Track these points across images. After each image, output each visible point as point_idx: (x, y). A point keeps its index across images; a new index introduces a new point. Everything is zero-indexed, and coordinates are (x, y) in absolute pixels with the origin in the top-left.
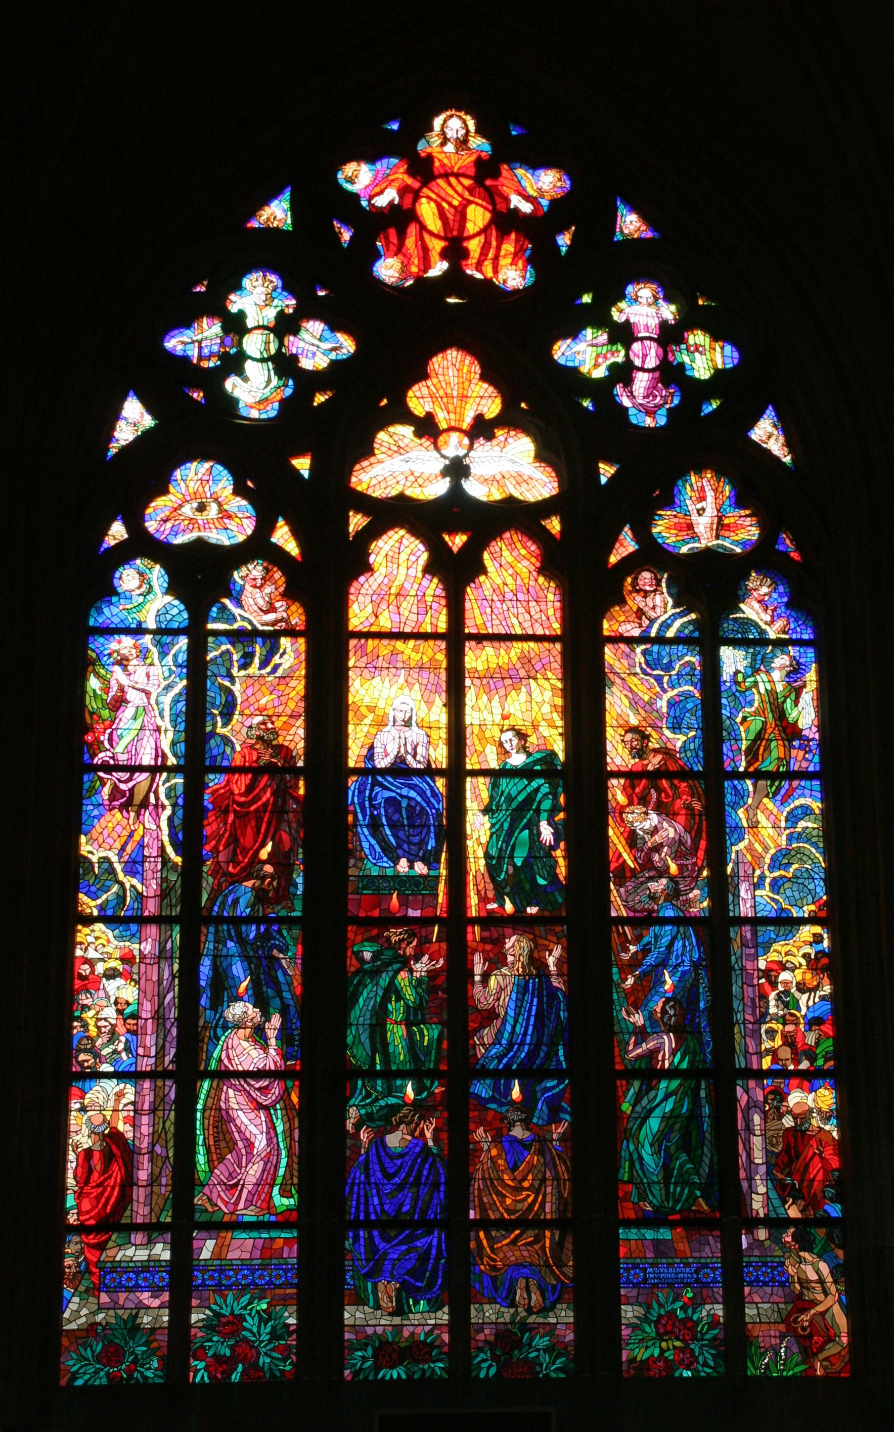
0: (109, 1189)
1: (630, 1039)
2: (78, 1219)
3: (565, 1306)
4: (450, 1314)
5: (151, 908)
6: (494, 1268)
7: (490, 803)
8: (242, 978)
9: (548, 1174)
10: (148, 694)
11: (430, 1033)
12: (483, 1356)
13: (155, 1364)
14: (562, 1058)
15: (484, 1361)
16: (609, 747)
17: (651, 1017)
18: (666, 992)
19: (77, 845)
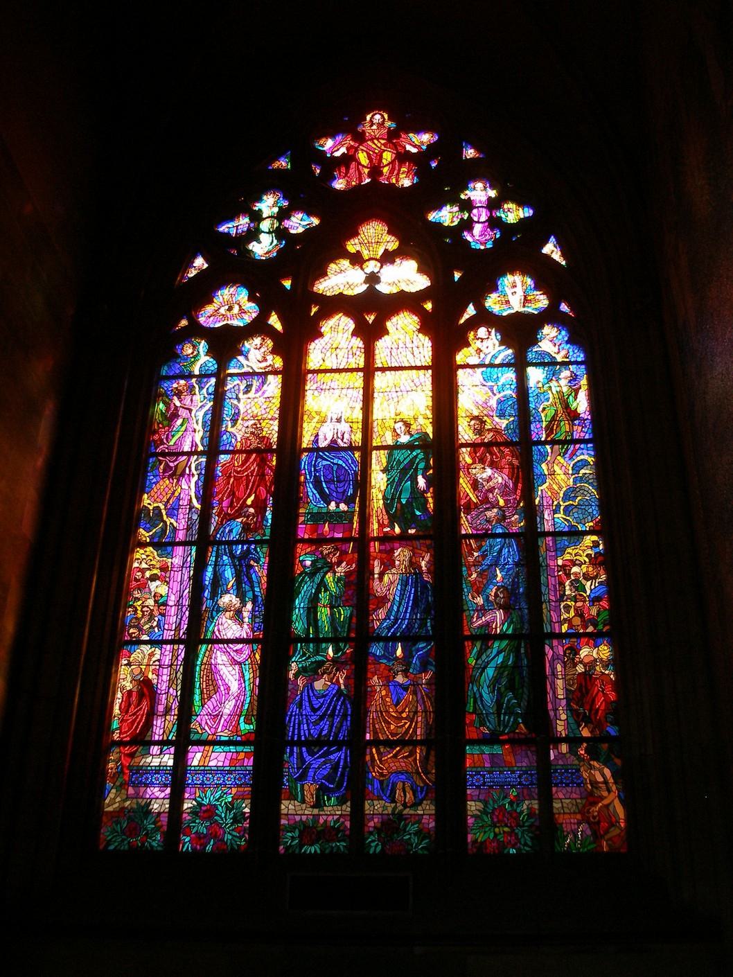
0: (140, 717)
1: (474, 615)
2: (119, 737)
3: (429, 802)
4: (351, 807)
5: (181, 536)
6: (381, 775)
7: (387, 466)
8: (231, 579)
9: (419, 708)
10: (190, 411)
11: (344, 613)
12: (371, 838)
13: (159, 837)
14: (429, 628)
15: (373, 841)
16: (460, 429)
17: (487, 600)
18: (498, 582)
19: (141, 500)
